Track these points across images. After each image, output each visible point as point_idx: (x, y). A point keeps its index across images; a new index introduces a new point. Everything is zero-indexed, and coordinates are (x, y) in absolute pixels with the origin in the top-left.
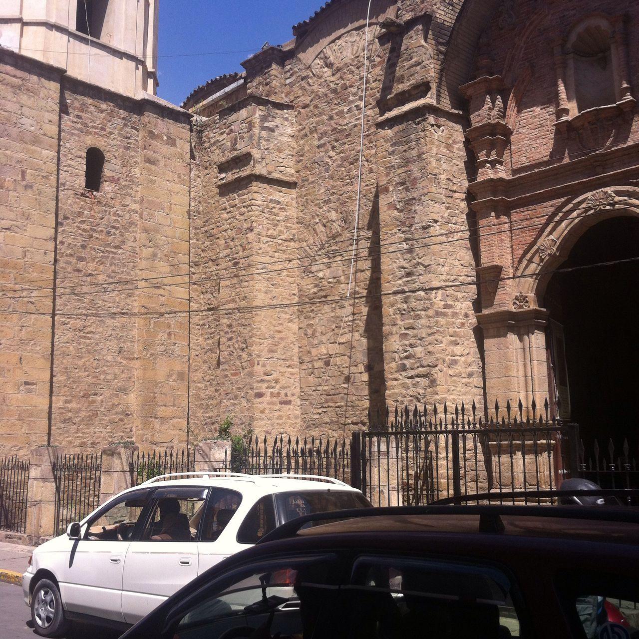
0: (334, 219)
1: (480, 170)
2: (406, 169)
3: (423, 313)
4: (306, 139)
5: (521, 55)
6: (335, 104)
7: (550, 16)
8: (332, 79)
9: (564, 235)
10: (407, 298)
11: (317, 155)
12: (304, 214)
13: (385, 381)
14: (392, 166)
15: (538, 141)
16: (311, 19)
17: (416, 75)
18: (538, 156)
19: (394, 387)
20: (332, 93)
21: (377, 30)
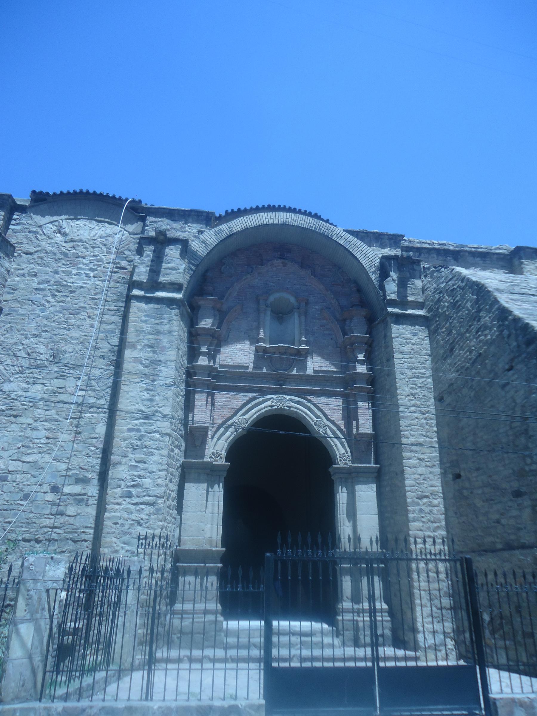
0: (42, 352)
1: (201, 357)
2: (156, 337)
3: (156, 451)
4: (23, 278)
5: (235, 295)
6: (64, 264)
7: (257, 280)
8: (64, 245)
11: (33, 294)
12: (5, 338)
13: (106, 504)
14: (143, 331)
16: (55, 194)
17: (171, 275)
18: (240, 362)
19: (116, 511)
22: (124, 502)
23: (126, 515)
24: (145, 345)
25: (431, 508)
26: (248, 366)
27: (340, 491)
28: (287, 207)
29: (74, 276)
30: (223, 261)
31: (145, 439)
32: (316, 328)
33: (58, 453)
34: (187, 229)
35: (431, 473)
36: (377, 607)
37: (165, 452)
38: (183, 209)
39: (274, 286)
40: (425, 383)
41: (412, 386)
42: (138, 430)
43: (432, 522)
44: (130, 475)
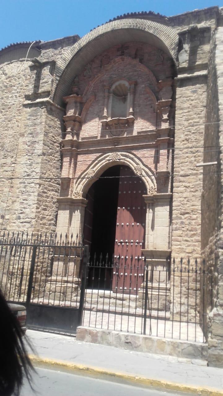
1: (67, 135)
2: (34, 127)
3: (32, 193)
5: (91, 90)
6: (6, 93)
7: (105, 76)
8: (6, 81)
10: (26, 186)
14: (28, 125)
15: (93, 128)
19: (13, 226)
20: (5, 87)
21: (30, 63)
22: (17, 222)
23: (17, 229)
24: (29, 133)
25: (190, 221)
26: (97, 137)
27: (148, 211)
28: (130, 14)
29: (10, 99)
30: (86, 68)
31: (27, 187)
33: (4, 198)
34: (63, 52)
36: (148, 285)
37: (36, 194)
38: (60, 39)
39: (115, 77)
40: (198, 129)
41: (186, 133)
42: (24, 183)
43: (190, 231)
44: (20, 207)
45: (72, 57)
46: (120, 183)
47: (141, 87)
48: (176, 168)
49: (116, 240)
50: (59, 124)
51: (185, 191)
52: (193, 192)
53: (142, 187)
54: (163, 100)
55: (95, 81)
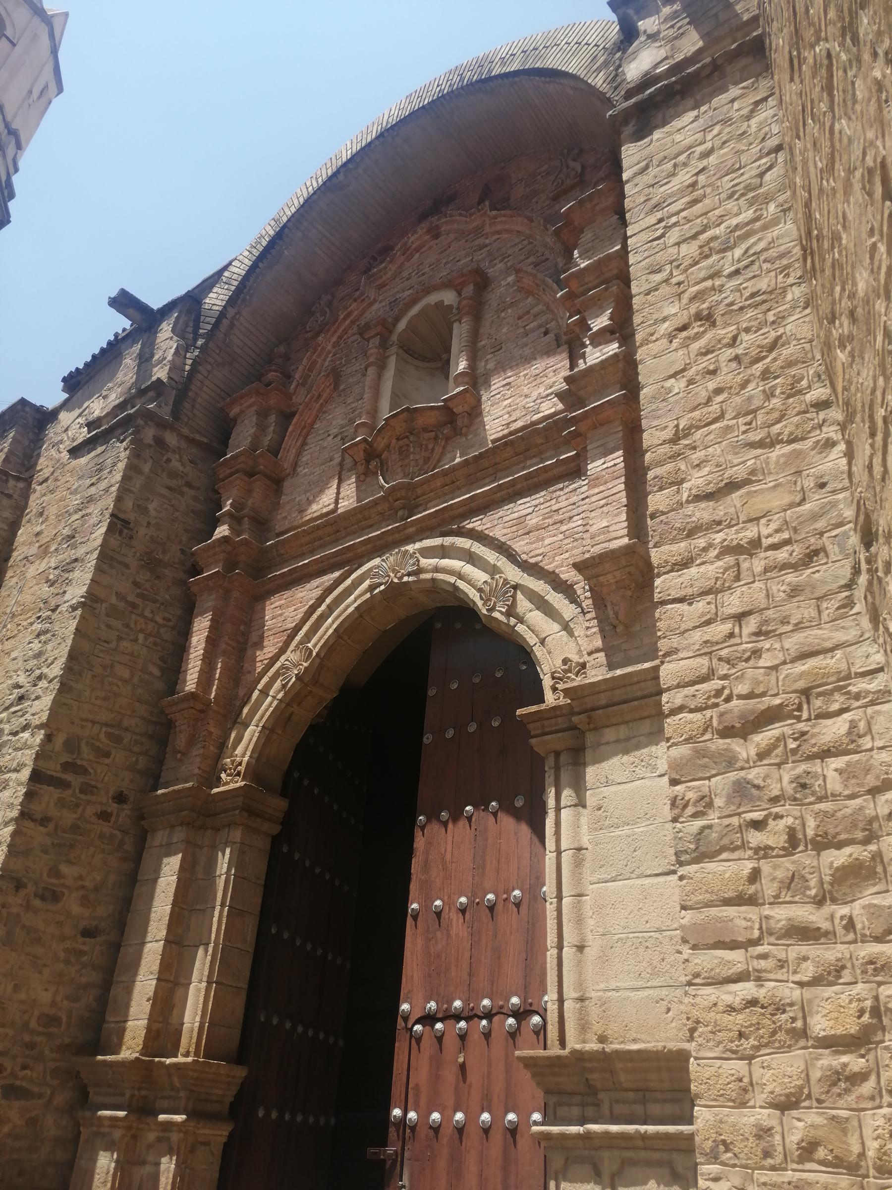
3: (14, 776)
5: (327, 363)
7: (376, 306)
9: (326, 637)
16: (87, 365)
30: (313, 309)
32: (504, 330)
35: (795, 591)
37: (26, 773)
45: (250, 263)
46: (432, 692)
47: (504, 286)
48: (660, 463)
49: (405, 1007)
50: (195, 498)
51: (731, 574)
52: (784, 566)
53: (515, 664)
54: (582, 266)
55: (342, 328)
